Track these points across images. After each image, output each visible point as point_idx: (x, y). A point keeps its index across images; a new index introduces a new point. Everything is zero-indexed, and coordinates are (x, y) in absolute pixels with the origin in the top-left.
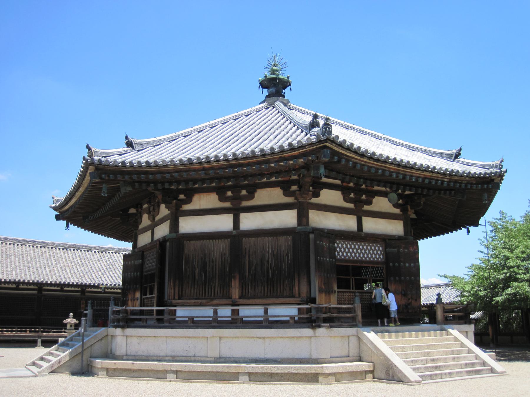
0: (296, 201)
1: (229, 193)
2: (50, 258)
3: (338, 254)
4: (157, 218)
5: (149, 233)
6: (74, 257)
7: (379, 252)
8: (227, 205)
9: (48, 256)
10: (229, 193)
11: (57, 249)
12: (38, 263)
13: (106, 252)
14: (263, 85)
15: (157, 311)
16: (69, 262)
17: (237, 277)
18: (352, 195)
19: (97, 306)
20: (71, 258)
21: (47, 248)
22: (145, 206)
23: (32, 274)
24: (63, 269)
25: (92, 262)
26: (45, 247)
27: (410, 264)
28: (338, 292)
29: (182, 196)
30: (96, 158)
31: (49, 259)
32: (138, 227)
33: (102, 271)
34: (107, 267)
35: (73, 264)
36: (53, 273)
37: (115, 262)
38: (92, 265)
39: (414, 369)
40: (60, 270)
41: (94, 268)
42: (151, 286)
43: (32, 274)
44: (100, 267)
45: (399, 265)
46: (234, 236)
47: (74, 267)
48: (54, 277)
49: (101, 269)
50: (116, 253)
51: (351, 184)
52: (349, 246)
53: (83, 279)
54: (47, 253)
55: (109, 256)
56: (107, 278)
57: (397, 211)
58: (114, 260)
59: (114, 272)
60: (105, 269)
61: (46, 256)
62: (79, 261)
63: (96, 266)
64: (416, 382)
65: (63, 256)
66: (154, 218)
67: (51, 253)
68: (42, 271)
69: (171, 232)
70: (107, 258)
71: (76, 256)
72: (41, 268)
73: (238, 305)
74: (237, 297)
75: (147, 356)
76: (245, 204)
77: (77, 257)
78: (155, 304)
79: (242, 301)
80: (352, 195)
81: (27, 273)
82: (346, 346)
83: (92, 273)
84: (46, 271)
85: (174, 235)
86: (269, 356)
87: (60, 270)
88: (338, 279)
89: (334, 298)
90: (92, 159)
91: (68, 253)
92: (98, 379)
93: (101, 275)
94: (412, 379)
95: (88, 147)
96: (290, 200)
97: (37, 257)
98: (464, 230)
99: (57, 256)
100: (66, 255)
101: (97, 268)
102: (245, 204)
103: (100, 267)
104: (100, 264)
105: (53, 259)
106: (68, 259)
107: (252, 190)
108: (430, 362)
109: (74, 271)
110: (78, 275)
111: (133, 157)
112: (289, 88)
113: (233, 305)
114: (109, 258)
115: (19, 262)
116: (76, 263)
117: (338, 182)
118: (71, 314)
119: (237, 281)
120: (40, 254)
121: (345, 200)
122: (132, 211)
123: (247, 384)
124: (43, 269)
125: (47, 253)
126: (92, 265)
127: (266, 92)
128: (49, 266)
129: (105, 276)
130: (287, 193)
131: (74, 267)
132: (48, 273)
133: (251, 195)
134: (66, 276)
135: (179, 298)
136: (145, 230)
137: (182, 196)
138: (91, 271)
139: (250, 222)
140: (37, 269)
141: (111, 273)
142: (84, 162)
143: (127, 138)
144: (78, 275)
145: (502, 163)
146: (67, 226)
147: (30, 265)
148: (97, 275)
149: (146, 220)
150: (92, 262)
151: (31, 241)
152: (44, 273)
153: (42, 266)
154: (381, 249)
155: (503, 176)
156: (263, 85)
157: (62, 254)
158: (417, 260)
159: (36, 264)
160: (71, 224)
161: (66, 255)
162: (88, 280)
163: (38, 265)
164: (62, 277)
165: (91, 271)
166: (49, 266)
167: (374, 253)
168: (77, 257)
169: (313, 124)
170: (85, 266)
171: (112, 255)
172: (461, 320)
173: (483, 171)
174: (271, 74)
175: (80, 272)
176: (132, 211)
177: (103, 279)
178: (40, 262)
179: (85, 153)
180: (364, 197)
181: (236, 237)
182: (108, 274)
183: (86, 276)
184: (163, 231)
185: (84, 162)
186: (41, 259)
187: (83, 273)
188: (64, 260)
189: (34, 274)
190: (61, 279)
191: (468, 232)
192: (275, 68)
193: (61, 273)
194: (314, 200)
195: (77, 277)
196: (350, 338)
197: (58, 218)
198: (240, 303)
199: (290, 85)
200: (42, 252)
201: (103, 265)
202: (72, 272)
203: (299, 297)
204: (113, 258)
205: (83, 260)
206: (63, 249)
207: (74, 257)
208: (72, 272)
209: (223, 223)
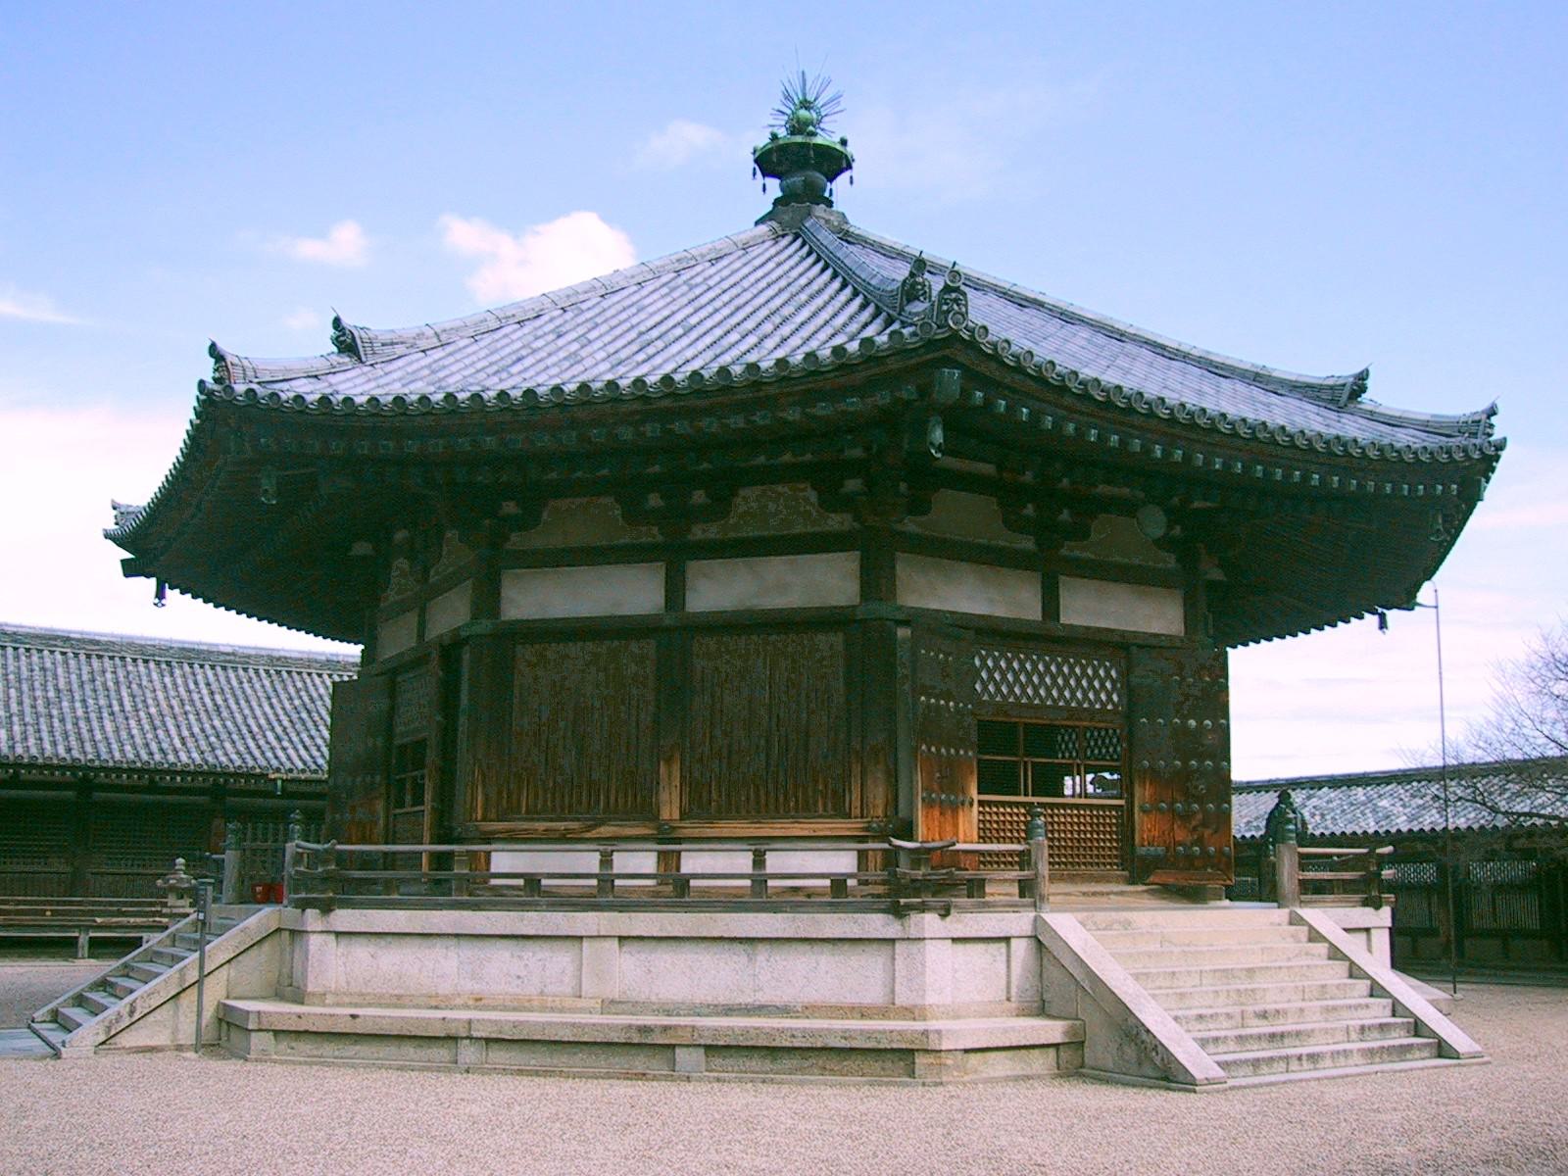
0: (856, 525)
2: (118, 691)
3: (985, 688)
5: (412, 618)
6: (192, 686)
7: (1108, 685)
9: (110, 684)
10: (654, 500)
11: (140, 662)
12: (78, 705)
13: (289, 672)
15: (434, 855)
16: (175, 703)
18: (1030, 510)
19: (255, 840)
20: (182, 690)
21: (106, 660)
22: (400, 536)
23: (59, 738)
24: (158, 723)
25: (247, 701)
26: (100, 657)
27: (1200, 723)
28: (981, 803)
29: (510, 508)
30: (240, 388)
31: (113, 694)
33: (279, 730)
34: (295, 716)
35: (188, 708)
36: (124, 735)
37: (319, 703)
38: (247, 712)
39: (1203, 1043)
40: (147, 727)
41: (251, 721)
42: (415, 779)
43: (59, 738)
44: (272, 717)
46: (668, 630)
47: (192, 717)
48: (128, 748)
49: (276, 724)
50: (320, 675)
51: (1028, 477)
52: (1016, 665)
53: (219, 752)
54: (109, 676)
55: (299, 685)
56: (291, 752)
58: (315, 695)
59: (313, 732)
60: (286, 723)
61: (104, 684)
62: (207, 700)
63: (258, 712)
64: (1209, 1081)
65: (158, 686)
66: (426, 571)
67: (121, 673)
68: (91, 731)
69: (475, 617)
70: (292, 690)
71: (196, 683)
72: (88, 720)
73: (679, 841)
74: (676, 816)
75: (399, 997)
76: (698, 533)
77: (202, 685)
78: (427, 836)
79: (690, 829)
80: (1030, 510)
81: (45, 735)
82: (1003, 967)
83: (248, 736)
84: (102, 728)
85: (485, 626)
86: (763, 998)
87: (147, 727)
88: (979, 761)
89: (969, 821)
90: (229, 389)
91: (172, 674)
92: (249, 1066)
93: (274, 743)
94: (1198, 1075)
95: (214, 351)
97: (75, 686)
98: (1371, 620)
99: (140, 685)
100: (167, 680)
101: (263, 722)
103: (272, 717)
104: (272, 706)
105: (124, 693)
106: (172, 693)
107: (724, 488)
108: (1256, 1022)
109: (190, 728)
110: (202, 743)
111: (357, 385)
112: (844, 177)
113: (660, 841)
114: (298, 691)
115: (20, 703)
116: (198, 704)
117: (987, 469)
118: (181, 860)
120: (85, 677)
121: (1008, 524)
122: (362, 548)
123: (699, 1080)
124: (95, 724)
125: (109, 676)
126: (247, 712)
127: (774, 188)
128: (112, 714)
129: (286, 744)
130: (833, 500)
131: (192, 717)
132: (111, 735)
133: (720, 504)
134: (165, 746)
136: (403, 608)
137: (510, 508)
138: (244, 730)
139: (719, 590)
140: (76, 724)
141: (304, 736)
142: (203, 397)
143: (337, 323)
144: (202, 743)
145: (1494, 420)
146: (160, 595)
147: (55, 712)
148: (262, 742)
150: (247, 701)
151: (56, 638)
152: (98, 736)
153: (93, 716)
154: (1113, 673)
155: (1497, 458)
157: (155, 676)
158: (1223, 710)
159: (73, 709)
160: (171, 588)
161: (167, 680)
162: (234, 757)
163: (80, 712)
164: (154, 747)
165: (244, 730)
166: (112, 714)
167: (1094, 688)
168: (202, 685)
169: (911, 290)
170: (225, 714)
172: (1356, 892)
173: (1433, 442)
174: (792, 133)
175: (209, 731)
176: (362, 548)
177: (280, 753)
178: (84, 701)
179: (207, 370)
180: (1065, 516)
181: (674, 635)
182: (295, 739)
183: (228, 745)
184: (451, 614)
185: (203, 397)
186: (88, 692)
187: (218, 737)
188: (161, 695)
189: (66, 737)
190: (151, 754)
191: (1383, 625)
192: (803, 113)
193: (150, 736)
194: (911, 526)
195: (198, 747)
196: (1013, 942)
197: (130, 569)
198: (687, 833)
199: (849, 167)
200: (92, 673)
201: (280, 712)
202: (186, 733)
204: (312, 689)
205: (218, 698)
206: (158, 663)
207: (192, 686)
208: (186, 733)
209: (633, 592)
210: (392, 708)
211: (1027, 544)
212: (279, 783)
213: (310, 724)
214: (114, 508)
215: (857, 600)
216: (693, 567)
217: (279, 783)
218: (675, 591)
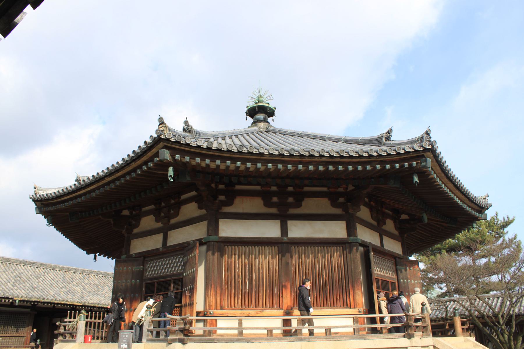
0: (344, 213)
1: (275, 199)
4: (173, 221)
5: (159, 237)
8: (274, 211)
14: (252, 112)
17: (289, 286)
27: (414, 281)
29: (222, 198)
32: (132, 231)
34: (15, 279)
45: (407, 281)
50: (20, 265)
55: (14, 268)
57: (396, 233)
60: (13, 281)
66: (169, 221)
69: (209, 234)
76: (292, 211)
96: (338, 211)
101: (5, 280)
102: (292, 211)
112: (272, 118)
119: (289, 291)
122: (126, 212)
133: (298, 204)
135: (222, 309)
143: (186, 122)
149: (148, 222)
156: (252, 112)
171: (20, 267)
177: (16, 291)
201: (10, 277)
203: (355, 308)
210: (143, 270)
211: (374, 223)
212: (17, 301)
213: (21, 282)
214: (35, 188)
215: (346, 237)
216: (290, 223)
217: (17, 301)
218: (284, 230)
